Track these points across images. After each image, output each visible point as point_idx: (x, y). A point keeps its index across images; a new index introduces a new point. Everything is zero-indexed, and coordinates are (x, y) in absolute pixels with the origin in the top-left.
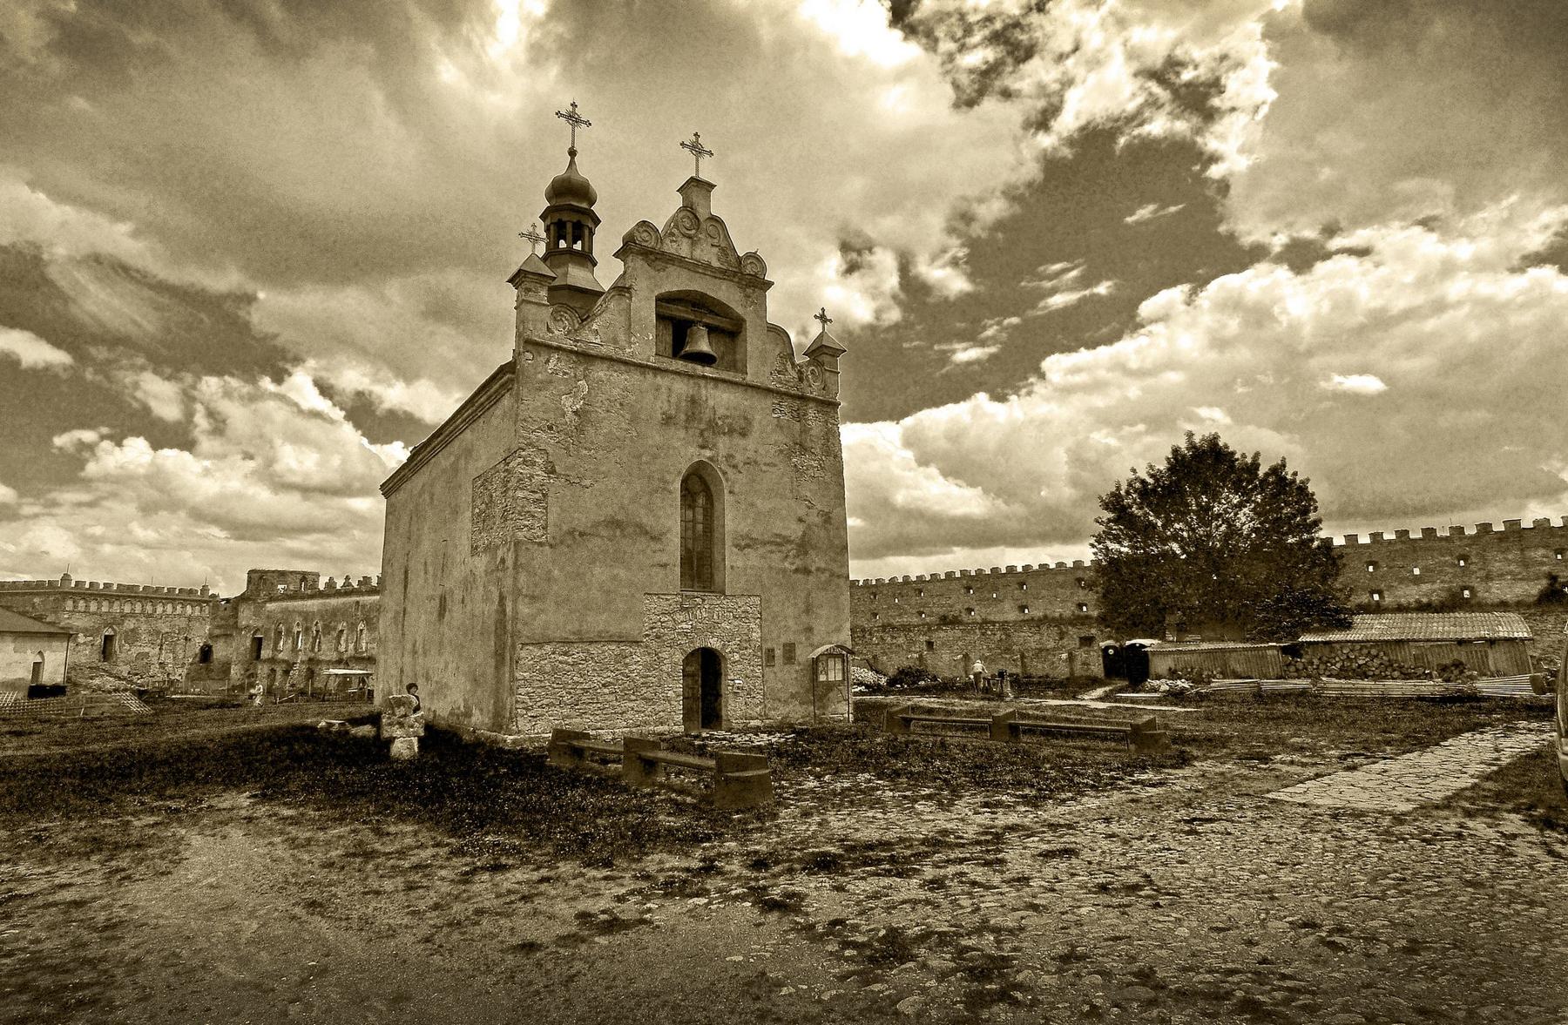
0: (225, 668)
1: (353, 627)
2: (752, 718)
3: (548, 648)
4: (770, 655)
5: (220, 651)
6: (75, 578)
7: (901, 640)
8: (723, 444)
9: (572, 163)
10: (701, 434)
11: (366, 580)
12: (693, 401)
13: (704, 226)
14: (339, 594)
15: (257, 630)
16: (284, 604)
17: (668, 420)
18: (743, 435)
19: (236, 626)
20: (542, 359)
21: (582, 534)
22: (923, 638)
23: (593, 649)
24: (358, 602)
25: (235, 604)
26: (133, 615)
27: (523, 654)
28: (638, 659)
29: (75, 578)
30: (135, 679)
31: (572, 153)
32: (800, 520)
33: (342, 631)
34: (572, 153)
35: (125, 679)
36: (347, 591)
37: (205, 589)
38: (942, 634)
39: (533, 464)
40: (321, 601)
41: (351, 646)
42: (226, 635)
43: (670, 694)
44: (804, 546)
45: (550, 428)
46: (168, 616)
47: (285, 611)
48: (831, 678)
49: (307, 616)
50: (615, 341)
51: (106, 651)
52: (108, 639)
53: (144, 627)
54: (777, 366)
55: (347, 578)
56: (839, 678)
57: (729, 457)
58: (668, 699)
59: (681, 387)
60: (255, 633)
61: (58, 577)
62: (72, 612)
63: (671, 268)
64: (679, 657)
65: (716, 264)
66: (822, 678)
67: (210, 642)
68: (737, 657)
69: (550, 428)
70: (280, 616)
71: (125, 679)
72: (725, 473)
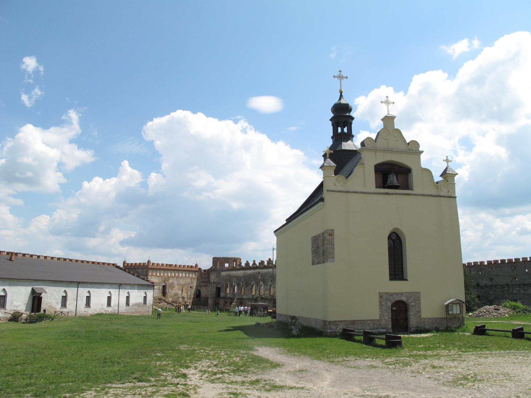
0: (207, 299)
1: (258, 284)
5: (204, 292)
6: (152, 262)
9: (341, 96)
11: (262, 262)
14: (251, 268)
15: (218, 283)
16: (228, 273)
19: (209, 281)
24: (259, 272)
25: (208, 272)
26: (172, 277)
29: (152, 262)
30: (174, 304)
31: (341, 93)
33: (253, 286)
34: (341, 93)
35: (170, 304)
36: (255, 267)
37: (196, 266)
41: (258, 292)
42: (205, 286)
43: (386, 318)
46: (184, 277)
47: (229, 276)
48: (455, 312)
49: (239, 278)
51: (164, 293)
52: (164, 287)
53: (176, 282)
55: (254, 261)
60: (216, 286)
61: (146, 262)
62: (152, 275)
64: (389, 304)
67: (200, 289)
68: (413, 304)
70: (227, 278)
71: (170, 304)
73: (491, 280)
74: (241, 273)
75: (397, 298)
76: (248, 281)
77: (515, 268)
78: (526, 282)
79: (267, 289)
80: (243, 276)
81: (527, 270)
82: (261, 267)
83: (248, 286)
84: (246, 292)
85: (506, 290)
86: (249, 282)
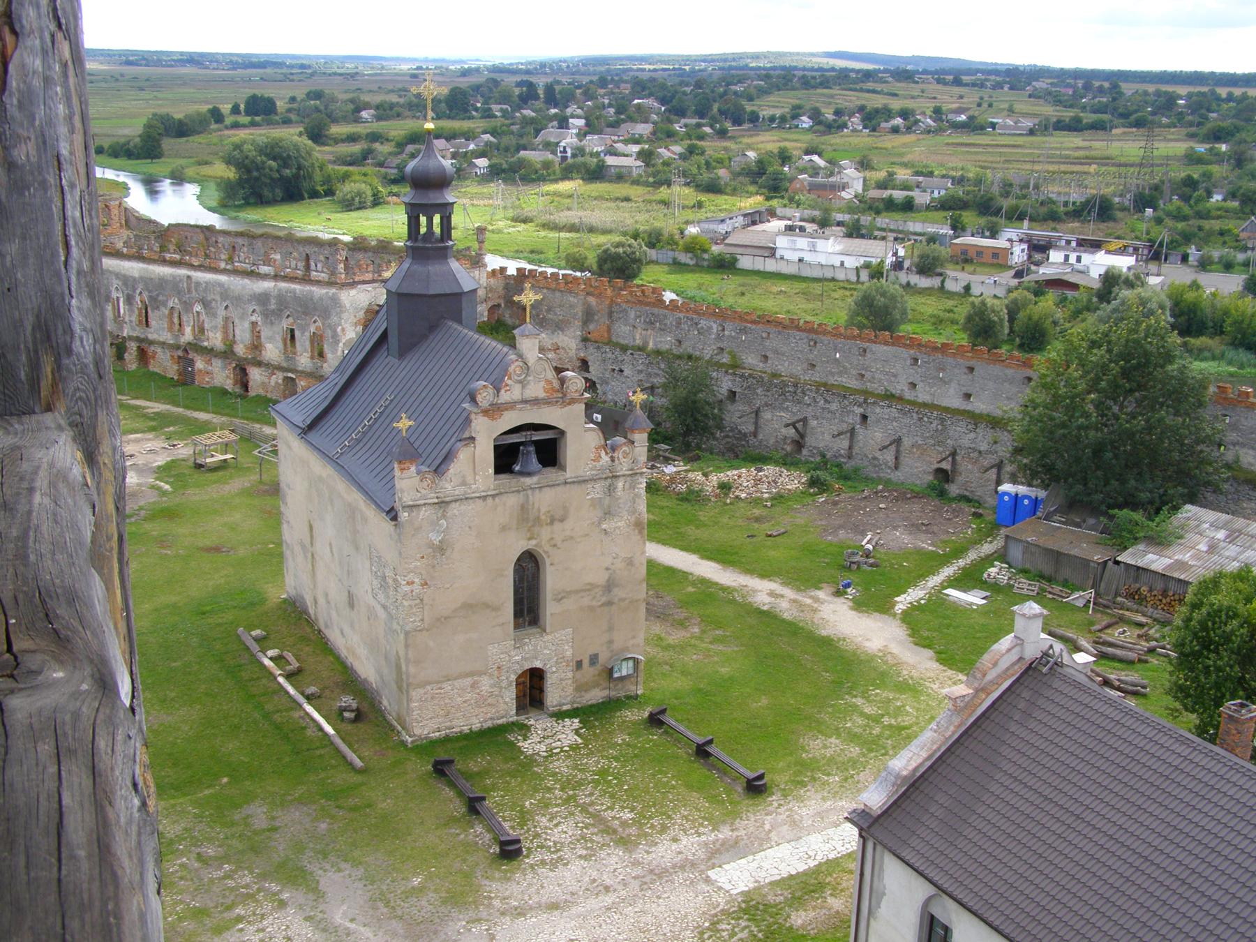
1: (188, 306)
2: (564, 704)
3: (429, 687)
4: (579, 664)
7: (834, 406)
8: (545, 533)
10: (529, 530)
12: (524, 508)
13: (532, 369)
17: (504, 528)
18: (562, 520)
20: (414, 514)
21: (446, 618)
22: (859, 411)
23: (456, 683)
24: (189, 277)
27: (414, 694)
28: (486, 684)
32: (607, 569)
38: (878, 410)
39: (413, 583)
40: (141, 265)
43: (507, 700)
44: (609, 586)
45: (423, 557)
49: (128, 282)
50: (464, 483)
54: (592, 456)
56: (631, 672)
57: (552, 539)
58: (506, 703)
59: (512, 501)
63: (505, 413)
64: (513, 677)
65: (542, 394)
66: (616, 675)
68: (554, 669)
69: (423, 557)
72: (546, 552)
73: (766, 357)
74: (132, 268)
75: (527, 666)
76: (158, 295)
77: (815, 343)
78: (831, 380)
79: (216, 327)
80: (141, 278)
81: (838, 356)
82: (196, 264)
83: (157, 308)
84: (153, 323)
85: (789, 391)
86: (161, 298)
